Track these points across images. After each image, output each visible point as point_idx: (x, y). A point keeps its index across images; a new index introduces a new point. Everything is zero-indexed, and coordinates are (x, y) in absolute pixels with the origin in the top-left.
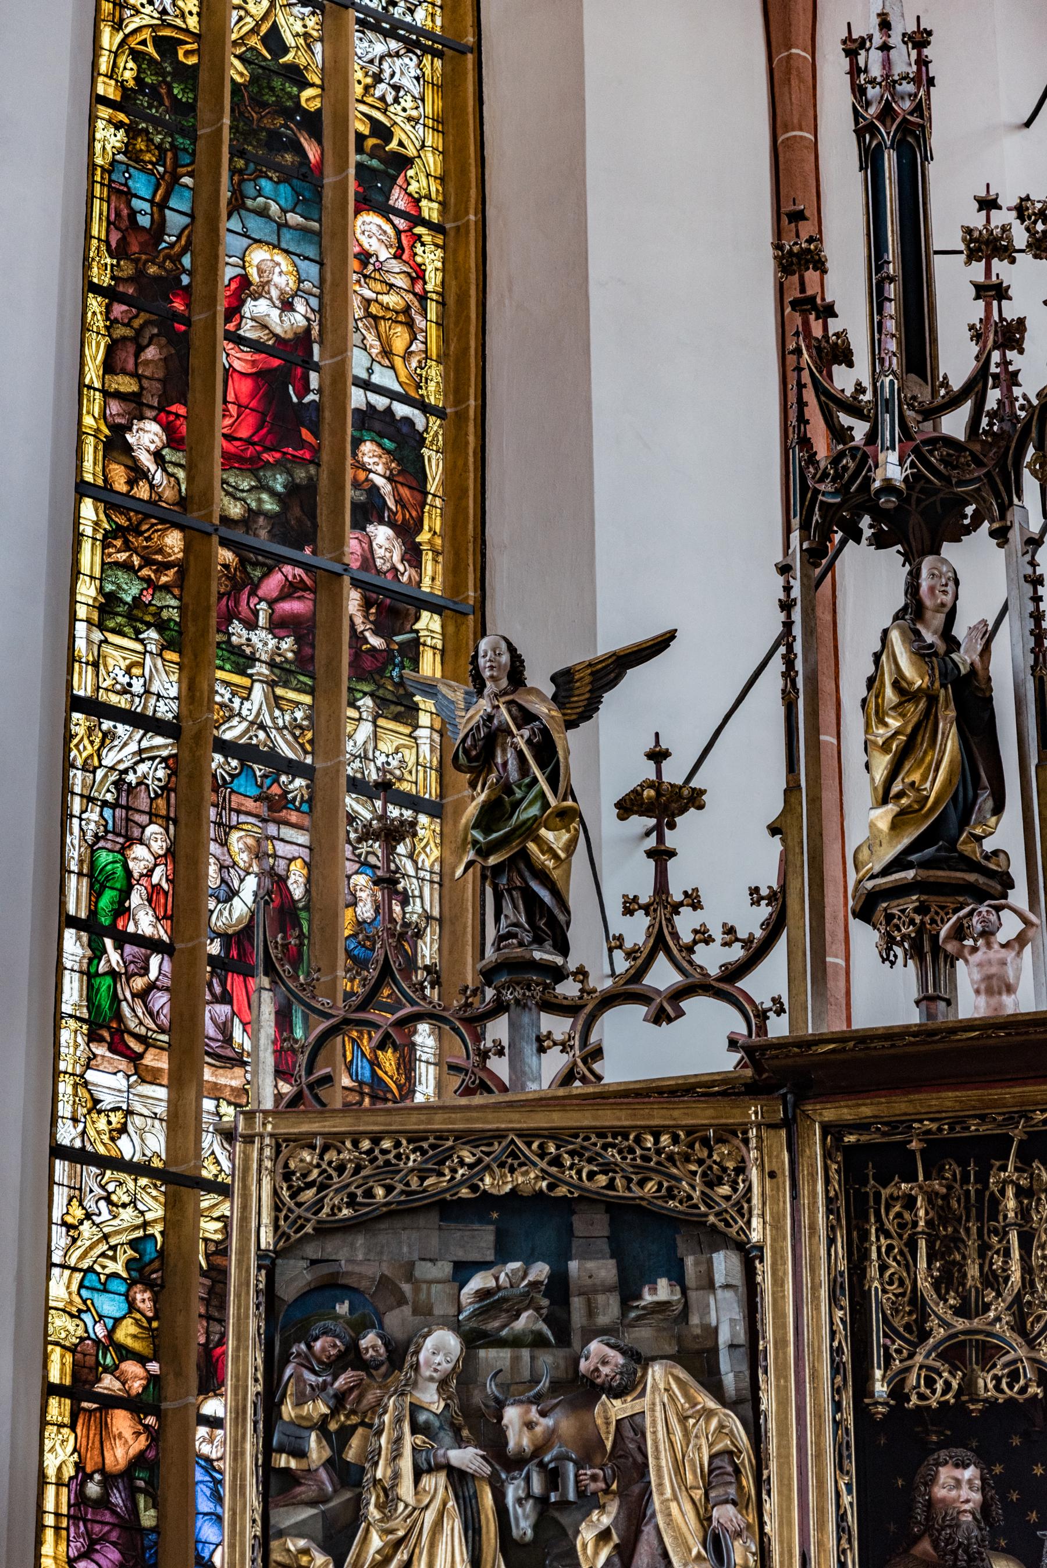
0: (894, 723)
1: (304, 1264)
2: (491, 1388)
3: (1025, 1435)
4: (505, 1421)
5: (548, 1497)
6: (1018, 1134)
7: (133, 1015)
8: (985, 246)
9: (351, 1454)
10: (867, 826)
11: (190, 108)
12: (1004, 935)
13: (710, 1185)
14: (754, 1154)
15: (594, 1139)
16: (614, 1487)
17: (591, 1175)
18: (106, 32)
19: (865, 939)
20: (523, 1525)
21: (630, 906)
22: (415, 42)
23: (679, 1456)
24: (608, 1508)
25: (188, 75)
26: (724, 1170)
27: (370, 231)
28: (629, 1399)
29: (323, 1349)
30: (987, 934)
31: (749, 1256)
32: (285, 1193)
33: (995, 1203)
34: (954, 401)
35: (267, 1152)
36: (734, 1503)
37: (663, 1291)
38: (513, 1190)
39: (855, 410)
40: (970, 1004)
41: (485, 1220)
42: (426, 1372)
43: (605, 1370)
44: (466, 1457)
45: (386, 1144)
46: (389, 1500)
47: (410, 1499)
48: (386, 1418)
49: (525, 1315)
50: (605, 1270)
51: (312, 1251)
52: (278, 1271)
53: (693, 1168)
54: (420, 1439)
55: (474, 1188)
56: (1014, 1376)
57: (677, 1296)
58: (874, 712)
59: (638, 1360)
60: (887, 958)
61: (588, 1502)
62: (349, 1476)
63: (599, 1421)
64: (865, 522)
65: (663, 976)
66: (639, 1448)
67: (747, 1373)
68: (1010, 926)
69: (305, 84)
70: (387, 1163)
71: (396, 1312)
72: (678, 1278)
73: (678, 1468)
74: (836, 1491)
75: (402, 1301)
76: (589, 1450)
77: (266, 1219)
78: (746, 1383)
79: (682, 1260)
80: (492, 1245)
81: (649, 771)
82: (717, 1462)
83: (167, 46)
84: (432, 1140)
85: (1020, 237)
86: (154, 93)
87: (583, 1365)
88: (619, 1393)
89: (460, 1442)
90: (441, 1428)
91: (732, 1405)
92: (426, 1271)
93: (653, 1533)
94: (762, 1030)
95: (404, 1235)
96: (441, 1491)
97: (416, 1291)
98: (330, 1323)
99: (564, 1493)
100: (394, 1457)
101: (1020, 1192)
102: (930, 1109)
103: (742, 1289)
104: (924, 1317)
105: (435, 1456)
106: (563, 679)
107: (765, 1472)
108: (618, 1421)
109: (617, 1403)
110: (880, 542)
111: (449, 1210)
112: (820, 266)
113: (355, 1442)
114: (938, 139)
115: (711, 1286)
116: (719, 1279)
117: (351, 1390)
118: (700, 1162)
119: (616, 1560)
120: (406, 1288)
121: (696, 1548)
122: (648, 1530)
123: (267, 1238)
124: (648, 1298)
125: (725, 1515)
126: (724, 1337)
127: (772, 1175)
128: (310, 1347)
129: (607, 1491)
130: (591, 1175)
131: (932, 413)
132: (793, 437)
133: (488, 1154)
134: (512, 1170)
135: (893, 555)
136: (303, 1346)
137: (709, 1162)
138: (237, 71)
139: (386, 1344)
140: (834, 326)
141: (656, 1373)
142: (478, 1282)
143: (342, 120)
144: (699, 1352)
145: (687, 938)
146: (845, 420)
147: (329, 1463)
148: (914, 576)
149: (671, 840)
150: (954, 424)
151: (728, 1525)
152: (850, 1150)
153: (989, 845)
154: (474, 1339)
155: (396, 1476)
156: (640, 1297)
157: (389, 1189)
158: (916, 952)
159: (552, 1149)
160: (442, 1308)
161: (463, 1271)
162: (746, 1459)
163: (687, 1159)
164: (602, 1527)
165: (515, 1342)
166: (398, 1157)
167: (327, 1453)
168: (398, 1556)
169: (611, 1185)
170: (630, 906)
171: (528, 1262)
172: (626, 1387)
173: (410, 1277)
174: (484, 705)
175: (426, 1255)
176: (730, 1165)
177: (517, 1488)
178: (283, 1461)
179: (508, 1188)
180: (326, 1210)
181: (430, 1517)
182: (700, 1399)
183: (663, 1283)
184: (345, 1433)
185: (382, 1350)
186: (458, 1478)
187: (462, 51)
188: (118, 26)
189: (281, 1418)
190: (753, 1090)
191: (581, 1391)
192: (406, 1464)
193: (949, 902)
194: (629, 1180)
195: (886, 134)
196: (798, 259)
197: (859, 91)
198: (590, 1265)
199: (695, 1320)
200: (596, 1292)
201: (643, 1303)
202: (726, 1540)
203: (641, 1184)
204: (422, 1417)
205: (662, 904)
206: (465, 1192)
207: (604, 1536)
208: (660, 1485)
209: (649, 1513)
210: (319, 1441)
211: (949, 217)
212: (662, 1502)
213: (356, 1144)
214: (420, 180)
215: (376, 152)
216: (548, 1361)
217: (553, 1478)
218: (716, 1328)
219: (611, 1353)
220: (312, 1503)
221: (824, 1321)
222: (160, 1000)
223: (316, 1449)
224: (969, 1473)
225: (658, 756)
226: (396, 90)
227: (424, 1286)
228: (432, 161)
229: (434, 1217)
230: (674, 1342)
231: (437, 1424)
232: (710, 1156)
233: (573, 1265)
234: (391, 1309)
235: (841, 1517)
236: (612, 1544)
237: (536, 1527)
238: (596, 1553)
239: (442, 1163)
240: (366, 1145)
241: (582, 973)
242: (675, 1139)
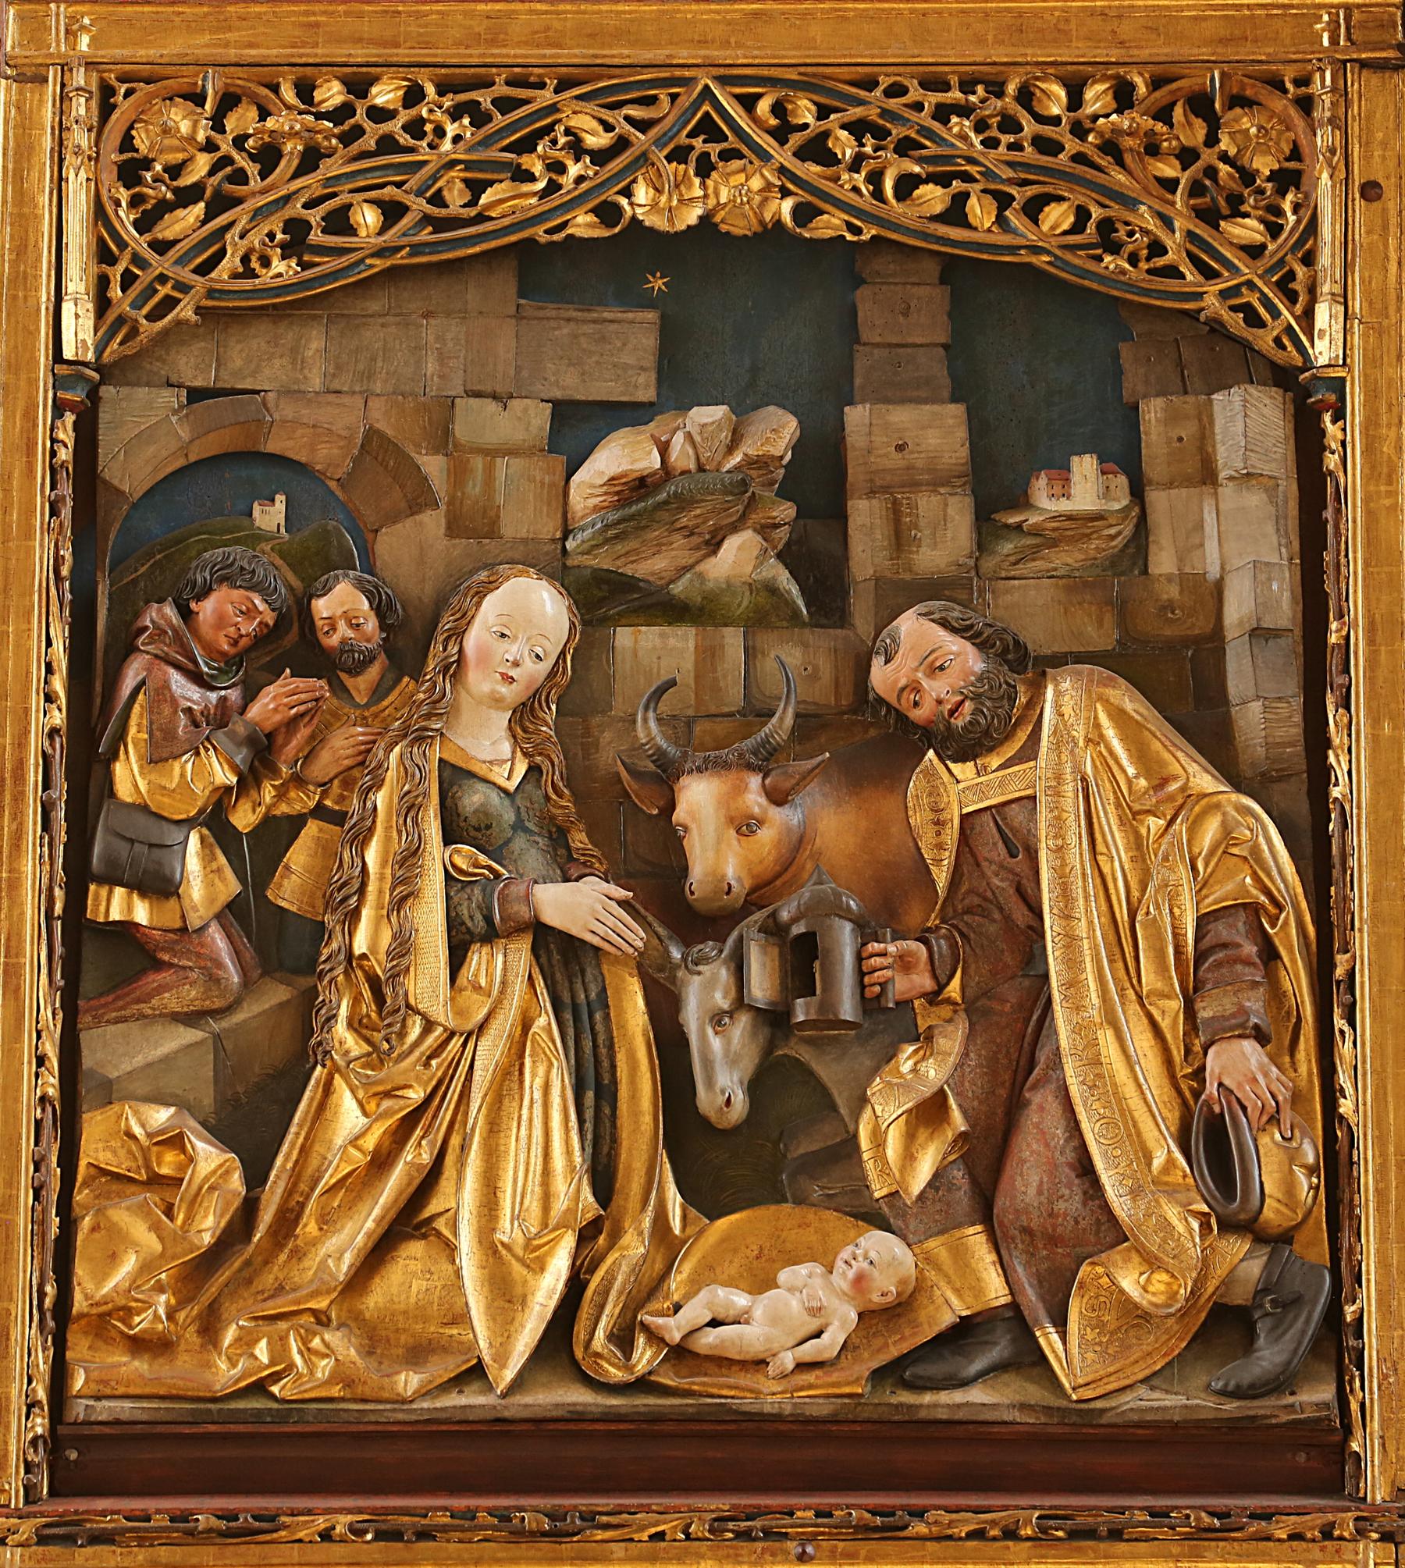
1: (172, 398)
2: (650, 731)
4: (679, 815)
5: (789, 1013)
13: (1210, 216)
14: (1324, 138)
15: (915, 93)
16: (954, 988)
17: (906, 186)
20: (724, 1085)
23: (1122, 914)
24: (941, 1042)
26: (1248, 177)
28: (995, 761)
29: (221, 621)
31: (1309, 403)
32: (126, 217)
35: (80, 107)
36: (1261, 1037)
37: (1086, 487)
38: (705, 219)
42: (479, 681)
43: (937, 688)
44: (582, 905)
45: (384, 94)
47: (441, 1013)
48: (381, 798)
49: (732, 546)
50: (938, 432)
52: (104, 416)
53: (1168, 169)
54: (464, 856)
55: (608, 213)
57: (1121, 500)
59: (1019, 663)
61: (888, 1023)
62: (284, 944)
63: (919, 819)
66: (1020, 891)
67: (1298, 702)
70: (387, 144)
71: (405, 527)
72: (1125, 458)
73: (1122, 943)
75: (420, 498)
77: (77, 283)
78: (1292, 728)
79: (1135, 408)
80: (650, 360)
82: (1221, 931)
84: (501, 89)
87: (882, 677)
90: (519, 826)
92: (480, 423)
93: (1054, 1107)
95: (429, 331)
96: (519, 987)
97: (458, 473)
98: (237, 552)
99: (828, 1005)
100: (401, 920)
103: (1290, 488)
105: (503, 899)
107: (1341, 959)
108: (964, 818)
109: (964, 771)
111: (540, 268)
113: (299, 856)
115: (1208, 475)
116: (1228, 457)
117: (292, 724)
118: (1187, 157)
119: (958, 1174)
120: (433, 466)
121: (1164, 1151)
123: (79, 332)
125: (1238, 1064)
126: (1237, 610)
127: (1371, 191)
128: (186, 614)
129: (933, 998)
130: (906, 186)
133: (643, 126)
134: (705, 169)
136: (170, 611)
137: (1208, 156)
139: (381, 609)
142: (618, 456)
144: (1173, 647)
147: (234, 913)
151: (1246, 1094)
154: (602, 601)
155: (403, 947)
156: (1023, 502)
157: (392, 212)
159: (805, 112)
160: (524, 518)
161: (577, 426)
163: (1153, 150)
164: (927, 1092)
166: (415, 128)
167: (231, 886)
168: (408, 1155)
169: (956, 214)
171: (744, 406)
172: (987, 733)
173: (442, 439)
175: (482, 382)
176: (1264, 165)
177: (709, 986)
178: (118, 905)
179: (692, 216)
180: (231, 262)
181: (489, 1053)
182: (1175, 768)
183: (1085, 467)
184: (278, 833)
185: (371, 625)
186: (561, 956)
189: (112, 794)
191: (880, 742)
192: (430, 918)
194: (1003, 201)
198: (902, 416)
199: (1163, 562)
200: (914, 485)
201: (1034, 519)
202: (1243, 1132)
203: (1033, 210)
204: (473, 799)
206: (583, 224)
207: (929, 1112)
208: (1073, 984)
209: (1042, 1057)
210: (207, 858)
212: (1077, 1030)
213: (305, 91)
216: (797, 664)
217: (803, 959)
218: (1219, 587)
219: (953, 644)
220: (191, 1018)
223: (202, 877)
227: (478, 463)
229: (504, 284)
230: (1109, 619)
231: (509, 816)
232: (1212, 140)
233: (856, 416)
234: (394, 518)
236: (950, 1135)
237: (755, 1087)
238: (909, 1157)
239: (526, 146)
240: (331, 94)
242: (1124, 96)
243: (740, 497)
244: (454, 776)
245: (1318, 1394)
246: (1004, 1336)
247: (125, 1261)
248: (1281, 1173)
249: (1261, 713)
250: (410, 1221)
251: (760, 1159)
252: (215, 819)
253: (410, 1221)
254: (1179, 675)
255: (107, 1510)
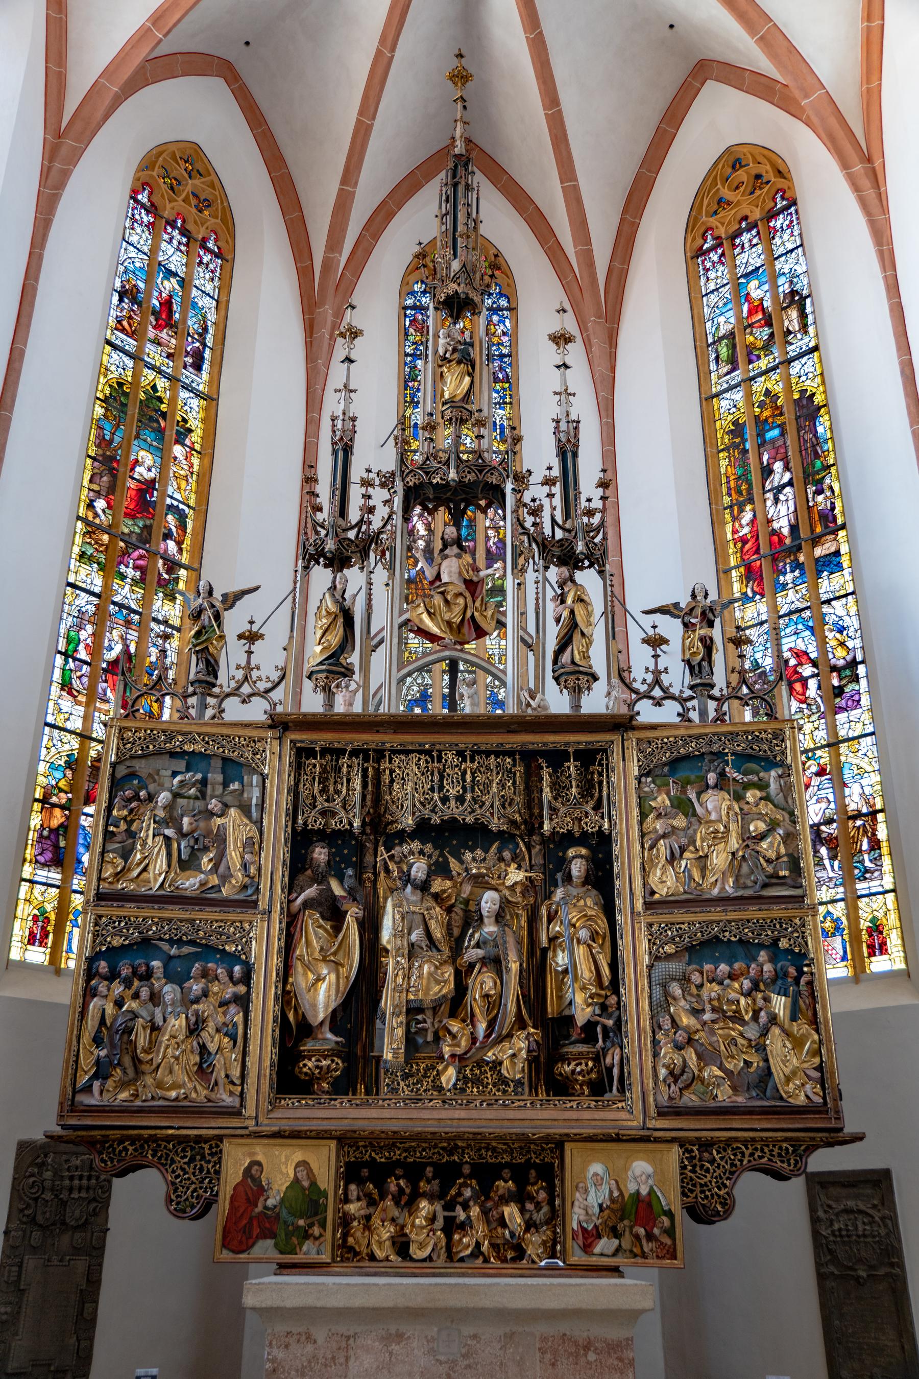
0: (324, 621)
3: (343, 841)
6: (349, 748)
7: (76, 684)
8: (366, 483)
9: (133, 828)
10: (315, 652)
11: (126, 405)
12: (350, 689)
18: (102, 377)
19: (308, 685)
21: (238, 667)
22: (198, 395)
25: (126, 394)
27: (178, 451)
30: (347, 687)
31: (264, 778)
33: (340, 769)
34: (352, 528)
37: (235, 786)
39: (323, 527)
40: (340, 707)
41: (183, 759)
46: (144, 843)
50: (220, 778)
51: (128, 763)
56: (341, 822)
58: (318, 616)
59: (226, 806)
60: (315, 691)
61: (206, 849)
62: (131, 834)
64: (321, 560)
65: (246, 689)
68: (353, 686)
69: (162, 403)
72: (242, 783)
73: (235, 842)
74: (283, 851)
75: (155, 781)
76: (208, 833)
81: (248, 626)
83: (120, 385)
85: (377, 482)
86: (115, 398)
88: (219, 816)
89: (168, 827)
91: (255, 823)
92: (163, 772)
94: (275, 709)
101: (348, 766)
102: (322, 739)
104: (315, 801)
106: (225, 596)
110: (326, 566)
111: (173, 755)
112: (316, 481)
113: (135, 824)
114: (355, 450)
122: (224, 860)
124: (232, 787)
126: (254, 801)
131: (345, 530)
132: (302, 532)
135: (329, 570)
138: (142, 396)
140: (318, 500)
141: (232, 811)
142: (178, 778)
143: (174, 415)
145: (254, 678)
146: (319, 529)
148: (335, 578)
149: (253, 648)
150: (351, 534)
152: (298, 749)
153: (349, 661)
154: (176, 795)
155: (147, 836)
158: (324, 689)
161: (175, 774)
162: (257, 840)
165: (189, 798)
170: (238, 667)
171: (196, 773)
174: (200, 601)
178: (111, 828)
181: (156, 850)
184: (132, 821)
186: (167, 839)
187: (213, 399)
188: (106, 376)
190: (270, 727)
192: (151, 833)
193: (336, 677)
195: (339, 446)
196: (310, 480)
197: (334, 432)
199: (245, 795)
205: (248, 668)
206: (178, 750)
207: (211, 860)
211: (357, 473)
214: (195, 437)
215: (182, 427)
217: (196, 840)
221: (285, 799)
222: (85, 680)
223: (123, 826)
224: (326, 850)
225: (252, 622)
226: (192, 409)
228: (199, 432)
235: (284, 861)
241: (221, 686)
243: (194, 785)
244: (155, 815)
245: (255, 897)
246: (217, 888)
247: (108, 872)
248: (252, 870)
249: (255, 814)
250: (145, 869)
251: (188, 864)
252: (125, 818)
253: (145, 869)
254: (245, 809)
255: (103, 903)
